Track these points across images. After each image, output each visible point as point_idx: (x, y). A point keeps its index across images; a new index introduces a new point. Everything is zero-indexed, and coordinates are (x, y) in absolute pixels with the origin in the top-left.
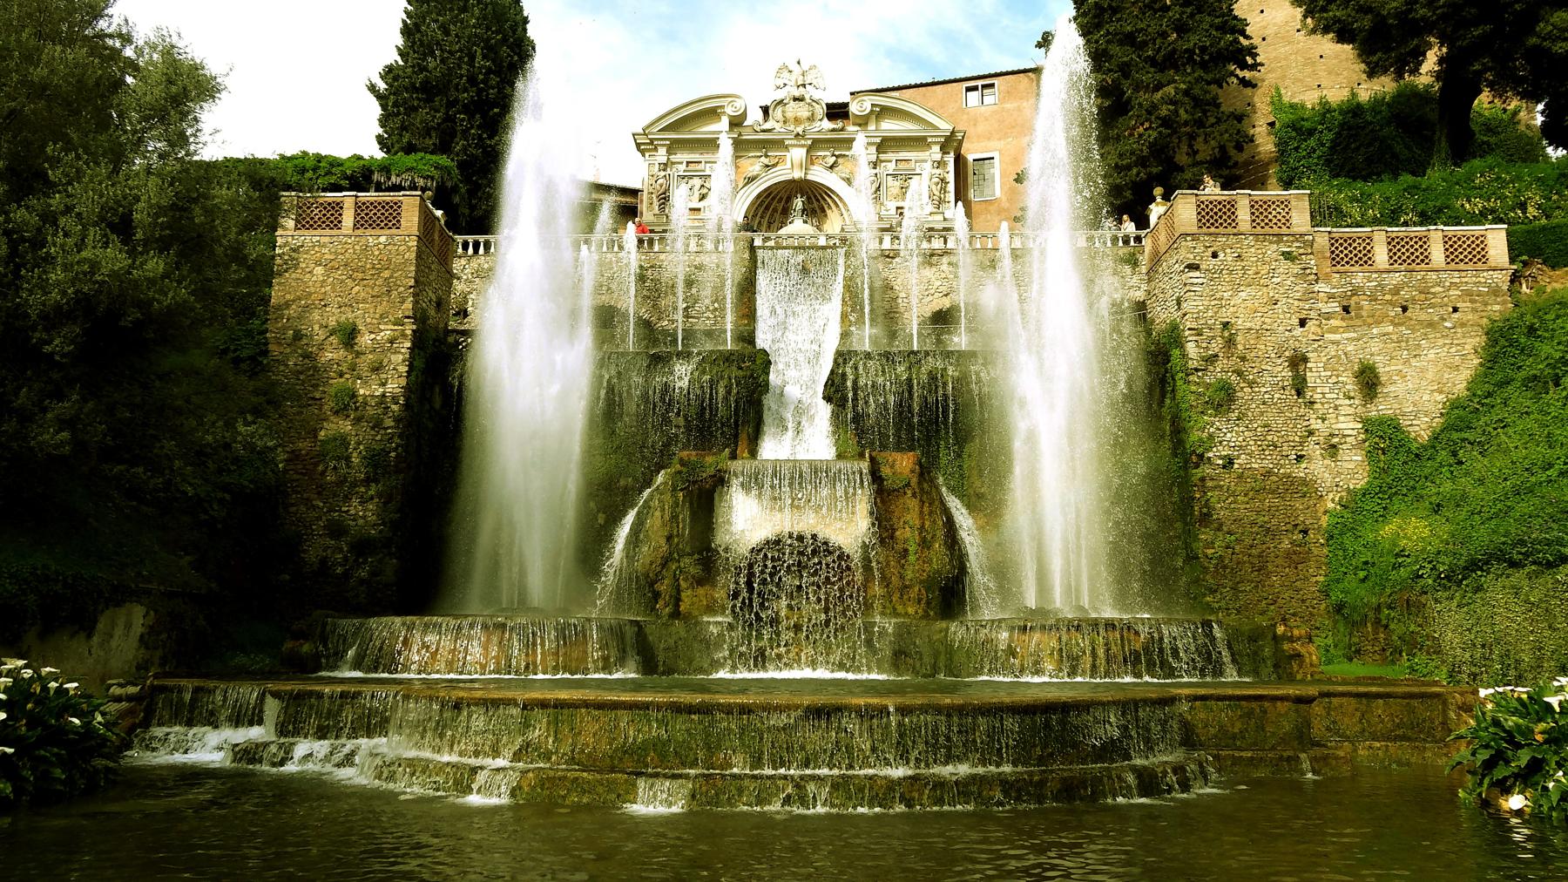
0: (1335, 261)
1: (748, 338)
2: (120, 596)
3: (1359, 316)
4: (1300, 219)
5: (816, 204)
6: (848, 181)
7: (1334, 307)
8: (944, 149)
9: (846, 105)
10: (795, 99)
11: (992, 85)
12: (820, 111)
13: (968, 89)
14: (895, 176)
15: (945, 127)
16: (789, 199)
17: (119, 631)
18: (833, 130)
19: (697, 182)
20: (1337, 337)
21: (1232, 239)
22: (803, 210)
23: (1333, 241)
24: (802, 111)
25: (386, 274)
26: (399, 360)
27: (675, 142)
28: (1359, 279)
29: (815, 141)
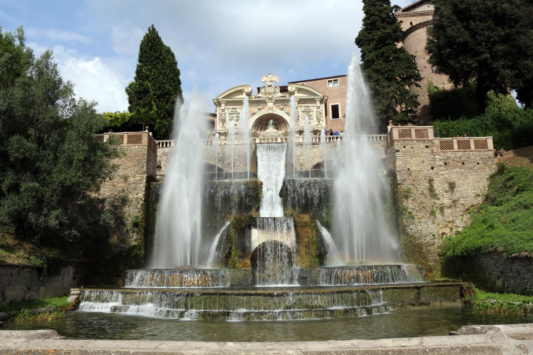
0: (442, 149)
3: (449, 166)
5: (277, 122)
6: (288, 114)
7: (442, 163)
10: (269, 86)
11: (337, 80)
12: (278, 90)
13: (329, 81)
14: (304, 112)
15: (321, 96)
17: (66, 275)
18: (282, 96)
19: (235, 115)
20: (443, 173)
21: (410, 142)
23: (441, 142)
24: (271, 90)
25: (138, 158)
28: (449, 154)
29: (276, 100)
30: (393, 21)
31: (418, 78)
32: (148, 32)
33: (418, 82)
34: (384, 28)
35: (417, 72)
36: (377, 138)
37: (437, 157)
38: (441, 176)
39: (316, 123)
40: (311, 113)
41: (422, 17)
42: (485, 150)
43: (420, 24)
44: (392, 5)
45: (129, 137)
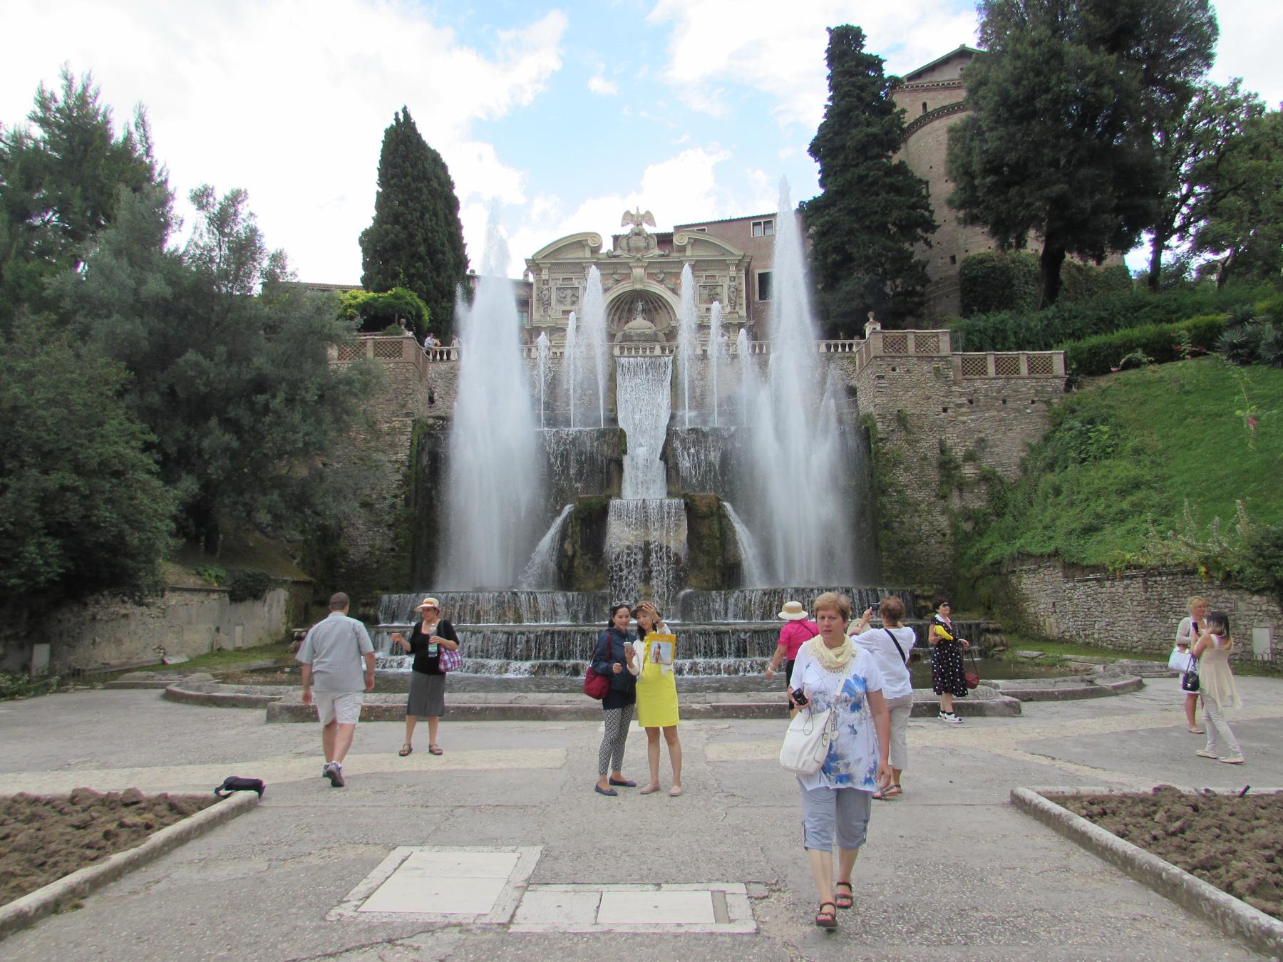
1: (614, 420)
2: (278, 584)
4: (945, 346)
6: (674, 291)
7: (964, 400)
9: (670, 235)
12: (654, 242)
14: (705, 287)
15: (739, 253)
19: (569, 292)
20: (964, 418)
22: (643, 310)
23: (964, 360)
25: (395, 386)
26: (405, 440)
28: (978, 384)
30: (886, 108)
31: (930, 226)
32: (394, 123)
34: (869, 124)
35: (927, 214)
36: (843, 346)
37: (954, 388)
39: (728, 309)
40: (718, 290)
41: (947, 93)
42: (1050, 375)
43: (943, 108)
44: (886, 74)
45: (377, 345)
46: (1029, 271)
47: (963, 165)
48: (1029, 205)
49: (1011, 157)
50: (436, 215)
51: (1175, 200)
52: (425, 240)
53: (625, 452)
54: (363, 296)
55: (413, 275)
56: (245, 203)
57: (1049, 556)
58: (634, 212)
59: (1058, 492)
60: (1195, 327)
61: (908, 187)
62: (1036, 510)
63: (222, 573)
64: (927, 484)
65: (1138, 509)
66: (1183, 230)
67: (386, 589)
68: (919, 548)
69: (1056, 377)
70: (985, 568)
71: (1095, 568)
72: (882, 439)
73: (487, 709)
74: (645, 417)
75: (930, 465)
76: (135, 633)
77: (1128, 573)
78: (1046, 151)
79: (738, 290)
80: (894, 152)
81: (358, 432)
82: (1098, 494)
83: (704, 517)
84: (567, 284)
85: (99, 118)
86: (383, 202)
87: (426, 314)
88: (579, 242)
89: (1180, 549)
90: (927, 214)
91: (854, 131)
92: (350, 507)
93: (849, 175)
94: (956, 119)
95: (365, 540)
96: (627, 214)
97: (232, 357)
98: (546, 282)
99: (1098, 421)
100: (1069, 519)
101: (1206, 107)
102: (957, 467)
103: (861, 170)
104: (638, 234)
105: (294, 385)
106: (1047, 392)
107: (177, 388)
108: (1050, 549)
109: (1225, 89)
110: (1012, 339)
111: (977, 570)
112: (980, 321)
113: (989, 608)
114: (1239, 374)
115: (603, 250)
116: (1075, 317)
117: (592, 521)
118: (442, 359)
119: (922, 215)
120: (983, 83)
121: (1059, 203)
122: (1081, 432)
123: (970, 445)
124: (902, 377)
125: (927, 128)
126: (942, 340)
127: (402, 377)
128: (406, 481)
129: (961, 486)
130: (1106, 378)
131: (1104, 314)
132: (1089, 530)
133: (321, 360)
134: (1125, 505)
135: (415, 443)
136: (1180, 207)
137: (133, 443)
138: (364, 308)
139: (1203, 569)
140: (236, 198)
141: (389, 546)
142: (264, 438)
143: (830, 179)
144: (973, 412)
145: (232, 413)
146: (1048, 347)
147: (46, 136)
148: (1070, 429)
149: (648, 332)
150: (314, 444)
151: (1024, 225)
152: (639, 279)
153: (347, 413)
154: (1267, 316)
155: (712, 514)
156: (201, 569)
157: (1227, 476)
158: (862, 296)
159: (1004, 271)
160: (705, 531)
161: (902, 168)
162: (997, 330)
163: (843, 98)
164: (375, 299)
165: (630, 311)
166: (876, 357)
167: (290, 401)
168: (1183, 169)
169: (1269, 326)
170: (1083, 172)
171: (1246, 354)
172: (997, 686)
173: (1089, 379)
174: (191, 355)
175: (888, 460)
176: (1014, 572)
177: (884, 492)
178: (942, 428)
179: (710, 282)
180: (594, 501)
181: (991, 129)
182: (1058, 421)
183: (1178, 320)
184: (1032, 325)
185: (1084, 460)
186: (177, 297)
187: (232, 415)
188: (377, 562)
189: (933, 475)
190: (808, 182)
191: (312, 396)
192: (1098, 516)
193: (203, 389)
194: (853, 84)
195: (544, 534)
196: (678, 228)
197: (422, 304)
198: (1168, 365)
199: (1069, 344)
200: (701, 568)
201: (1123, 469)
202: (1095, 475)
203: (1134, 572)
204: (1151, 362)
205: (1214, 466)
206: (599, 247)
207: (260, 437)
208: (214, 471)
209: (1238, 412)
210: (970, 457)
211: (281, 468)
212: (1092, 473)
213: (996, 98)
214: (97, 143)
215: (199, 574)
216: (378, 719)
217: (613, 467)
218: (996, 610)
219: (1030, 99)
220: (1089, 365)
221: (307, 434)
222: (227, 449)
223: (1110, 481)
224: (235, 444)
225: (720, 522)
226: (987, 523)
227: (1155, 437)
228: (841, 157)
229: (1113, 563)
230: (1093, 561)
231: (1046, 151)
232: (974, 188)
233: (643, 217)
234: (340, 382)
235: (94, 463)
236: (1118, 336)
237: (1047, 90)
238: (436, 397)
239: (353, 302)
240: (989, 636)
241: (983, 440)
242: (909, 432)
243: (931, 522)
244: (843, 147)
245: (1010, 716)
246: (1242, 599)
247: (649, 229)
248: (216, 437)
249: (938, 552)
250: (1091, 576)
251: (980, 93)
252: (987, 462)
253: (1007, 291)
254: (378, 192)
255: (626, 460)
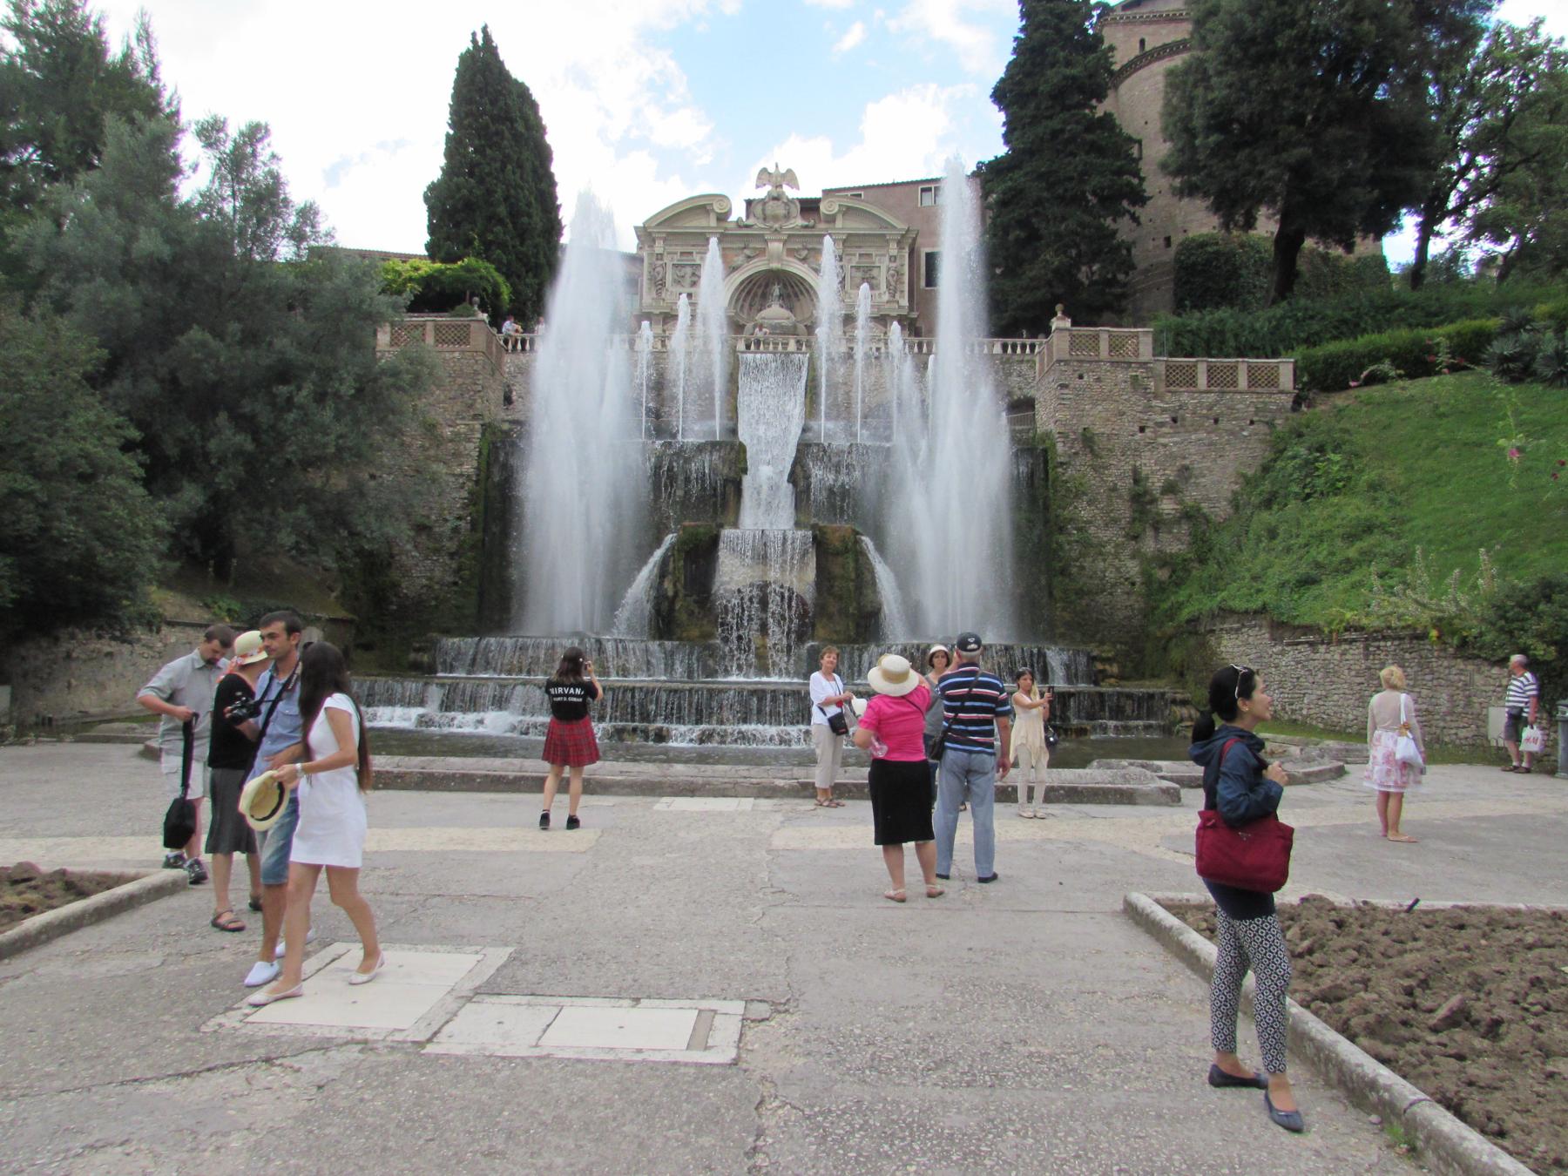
1: (734, 431)
6: (817, 271)
7: (1166, 418)
8: (901, 248)
9: (817, 201)
14: (858, 268)
15: (901, 226)
16: (767, 286)
19: (689, 270)
21: (1094, 366)
23: (1168, 368)
25: (460, 381)
26: (472, 448)
27: (669, 234)
28: (1185, 398)
31: (1139, 198)
33: (1138, 210)
34: (1068, 64)
35: (1135, 181)
36: (1023, 347)
37: (1154, 403)
38: (1161, 450)
39: (886, 297)
40: (875, 272)
43: (1164, 47)
45: (438, 328)
46: (1262, 259)
47: (1182, 120)
48: (1261, 173)
49: (1244, 110)
50: (520, 166)
51: (1450, 173)
52: (506, 199)
53: (745, 471)
54: (427, 267)
55: (491, 243)
56: (266, 141)
57: (1256, 612)
58: (772, 170)
59: (1272, 534)
60: (1459, 334)
61: (1112, 145)
62: (1246, 555)
63: (236, 606)
64: (1115, 521)
65: (1367, 557)
66: (1459, 211)
67: (448, 632)
68: (1101, 599)
69: (1282, 392)
70: (1180, 626)
71: (1307, 629)
72: (1062, 464)
73: (522, 778)
74: (770, 428)
75: (1120, 497)
76: (122, 675)
77: (1347, 636)
78: (1286, 103)
79: (899, 273)
80: (1100, 101)
81: (413, 434)
82: (1320, 537)
83: (837, 554)
84: (686, 260)
85: (91, 28)
86: (454, 148)
87: (506, 292)
88: (700, 207)
89: (1409, 608)
90: (1135, 181)
91: (1050, 73)
92: (400, 531)
93: (1040, 130)
94: (1178, 61)
95: (421, 571)
96: (764, 170)
97: (251, 338)
98: (660, 256)
99: (1329, 448)
100: (1283, 569)
101: (1497, 54)
102: (1153, 501)
103: (1055, 124)
104: (776, 199)
105: (327, 374)
106: (1271, 411)
107: (179, 374)
108: (1256, 604)
109: (1523, 31)
110: (1232, 343)
111: (1169, 627)
112: (1194, 320)
113: (1182, 674)
114: (1509, 395)
115: (733, 218)
116: (1312, 318)
117: (698, 556)
118: (523, 349)
119: (1129, 184)
120: (1212, 12)
121: (1300, 171)
122: (1307, 463)
123: (1171, 473)
124: (1089, 387)
125: (1143, 73)
126: (1142, 341)
127: (468, 370)
128: (473, 499)
129: (1158, 525)
130: (1344, 394)
131: (1348, 315)
132: (1306, 582)
133: (361, 345)
134: (1352, 553)
135: (485, 452)
136: (1457, 181)
137: (108, 440)
138: (428, 281)
139: (1434, 633)
140: (255, 134)
141: (449, 579)
142: (287, 438)
143: (1017, 134)
144: (1172, 435)
145: (247, 407)
146: (1275, 354)
147: (23, 50)
148: (1294, 457)
149: (785, 322)
150: (350, 449)
151: (1257, 198)
152: (777, 257)
153: (393, 412)
154: (1552, 323)
155: (847, 550)
156: (209, 601)
157: (1479, 521)
158: (1049, 284)
159: (1229, 256)
160: (837, 571)
161: (1107, 122)
162: (1213, 331)
163: (1036, 30)
164: (441, 272)
165: (764, 296)
166: (1059, 361)
167: (320, 397)
168: (1465, 133)
169: (1550, 334)
170: (1334, 132)
171: (1518, 370)
172: (1159, 769)
173: (1323, 396)
174: (196, 333)
175: (1068, 490)
176: (1213, 631)
177: (1061, 530)
178: (1137, 453)
179: (865, 262)
180: (702, 530)
181: (1220, 73)
182: (1281, 446)
183: (1438, 324)
184: (1258, 325)
185: (1309, 496)
186: (177, 258)
187: (247, 410)
188: (436, 598)
189: (1123, 510)
190: (988, 138)
191: (347, 389)
192: (1318, 565)
193: (212, 377)
194: (1051, 12)
195: (639, 570)
196: (826, 192)
197: (500, 279)
198: (1421, 381)
199: (1301, 351)
200: (830, 617)
201: (1353, 508)
202: (1319, 515)
203: (1354, 635)
204: (1400, 377)
205: (1465, 506)
206: (728, 214)
207: (281, 440)
208: (223, 480)
209: (1501, 442)
210: (1170, 489)
211: (315, 479)
212: (1316, 513)
213: (1227, 33)
214: (86, 58)
215: (207, 606)
216: (387, 787)
217: (730, 489)
218: (1190, 677)
219: (1269, 36)
220: (1324, 379)
221: (341, 436)
222: (239, 453)
223: (1338, 522)
224: (249, 446)
225: (857, 561)
226: (1188, 571)
227: (1397, 470)
228: (1033, 105)
229: (1330, 623)
230: (1307, 620)
231: (1286, 103)
232: (1194, 149)
233: (783, 176)
234: (383, 372)
235: (53, 464)
236: (1362, 342)
237: (1292, 24)
238: (514, 396)
239: (415, 274)
240: (1176, 709)
241: (1187, 468)
242: (1096, 456)
243: (1117, 567)
244: (1034, 93)
245: (1167, 804)
246: (1479, 672)
247: (790, 193)
248: (227, 437)
249: (1124, 604)
250: (1303, 639)
251: (1208, 26)
252: (1191, 495)
253: (1233, 283)
254: (448, 135)
255: (747, 481)
